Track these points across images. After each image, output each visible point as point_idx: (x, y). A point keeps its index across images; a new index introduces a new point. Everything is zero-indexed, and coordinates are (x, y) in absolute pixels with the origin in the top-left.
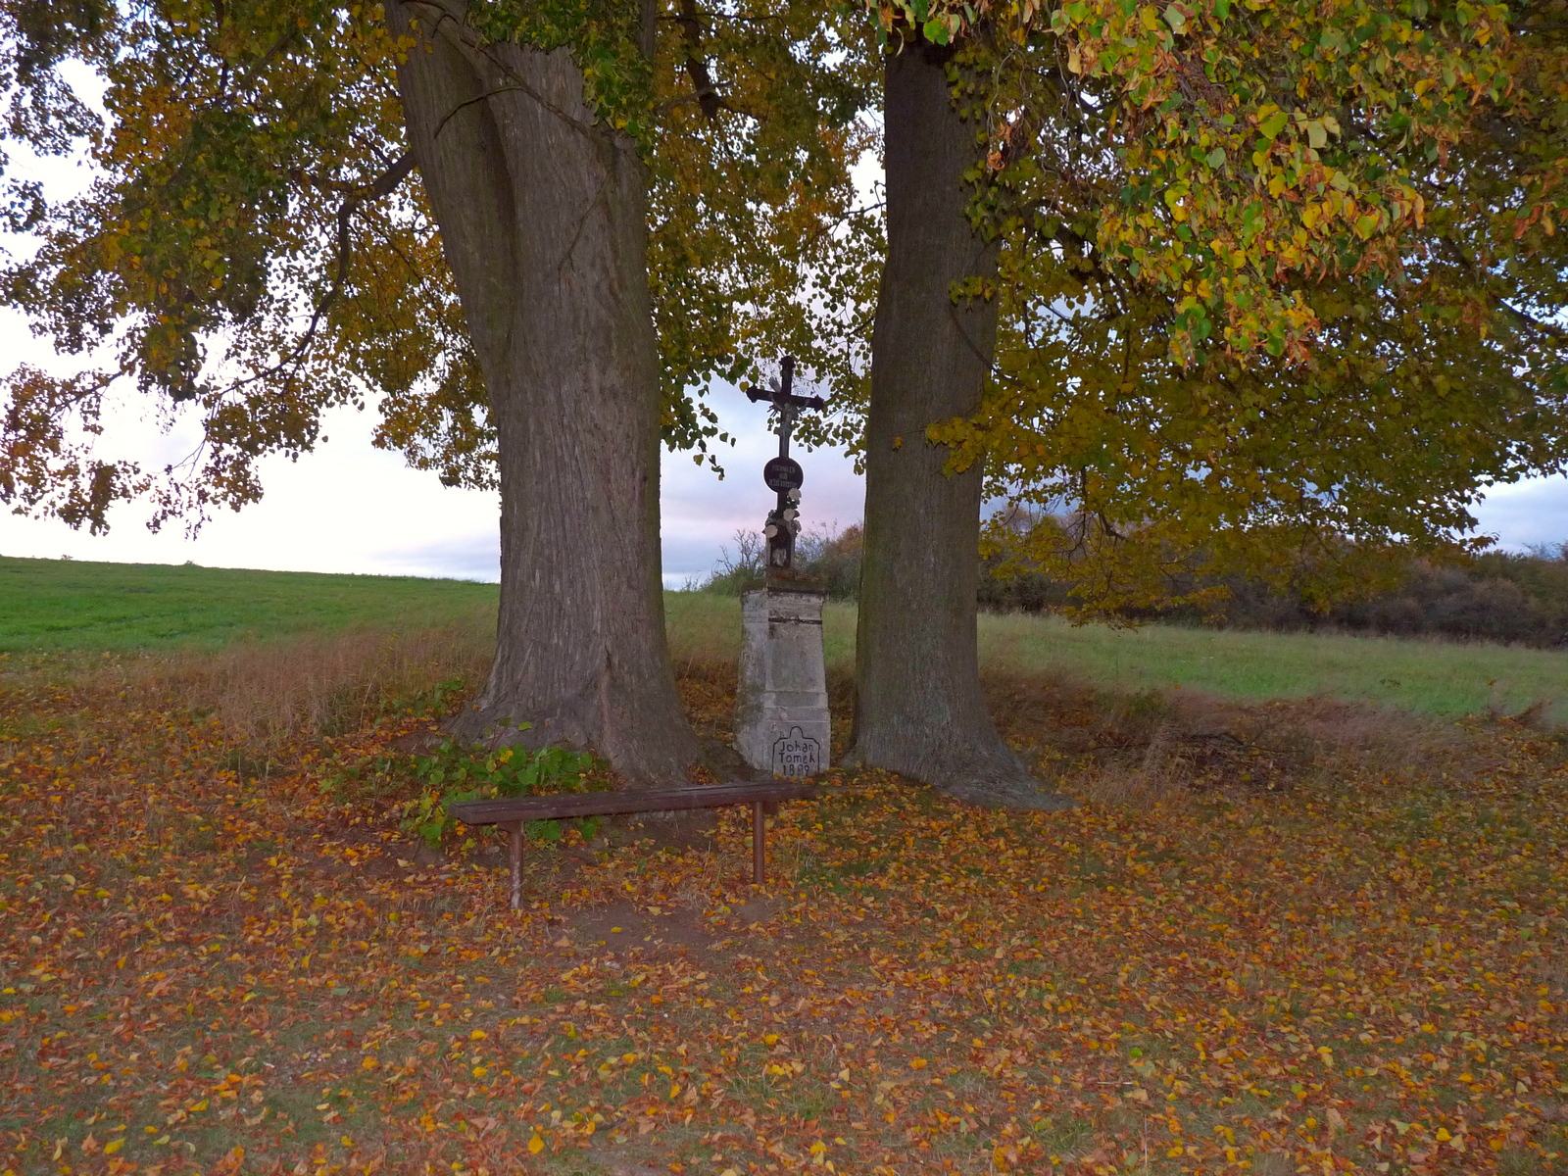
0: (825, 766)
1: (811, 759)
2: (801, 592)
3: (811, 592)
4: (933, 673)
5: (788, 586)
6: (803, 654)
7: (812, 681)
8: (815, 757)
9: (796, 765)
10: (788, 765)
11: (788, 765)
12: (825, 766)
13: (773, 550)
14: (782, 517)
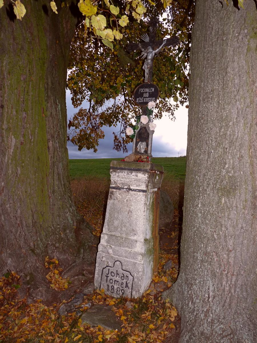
2: (131, 170)
3: (138, 170)
5: (122, 166)
6: (130, 212)
8: (130, 285)
9: (116, 287)
10: (110, 285)
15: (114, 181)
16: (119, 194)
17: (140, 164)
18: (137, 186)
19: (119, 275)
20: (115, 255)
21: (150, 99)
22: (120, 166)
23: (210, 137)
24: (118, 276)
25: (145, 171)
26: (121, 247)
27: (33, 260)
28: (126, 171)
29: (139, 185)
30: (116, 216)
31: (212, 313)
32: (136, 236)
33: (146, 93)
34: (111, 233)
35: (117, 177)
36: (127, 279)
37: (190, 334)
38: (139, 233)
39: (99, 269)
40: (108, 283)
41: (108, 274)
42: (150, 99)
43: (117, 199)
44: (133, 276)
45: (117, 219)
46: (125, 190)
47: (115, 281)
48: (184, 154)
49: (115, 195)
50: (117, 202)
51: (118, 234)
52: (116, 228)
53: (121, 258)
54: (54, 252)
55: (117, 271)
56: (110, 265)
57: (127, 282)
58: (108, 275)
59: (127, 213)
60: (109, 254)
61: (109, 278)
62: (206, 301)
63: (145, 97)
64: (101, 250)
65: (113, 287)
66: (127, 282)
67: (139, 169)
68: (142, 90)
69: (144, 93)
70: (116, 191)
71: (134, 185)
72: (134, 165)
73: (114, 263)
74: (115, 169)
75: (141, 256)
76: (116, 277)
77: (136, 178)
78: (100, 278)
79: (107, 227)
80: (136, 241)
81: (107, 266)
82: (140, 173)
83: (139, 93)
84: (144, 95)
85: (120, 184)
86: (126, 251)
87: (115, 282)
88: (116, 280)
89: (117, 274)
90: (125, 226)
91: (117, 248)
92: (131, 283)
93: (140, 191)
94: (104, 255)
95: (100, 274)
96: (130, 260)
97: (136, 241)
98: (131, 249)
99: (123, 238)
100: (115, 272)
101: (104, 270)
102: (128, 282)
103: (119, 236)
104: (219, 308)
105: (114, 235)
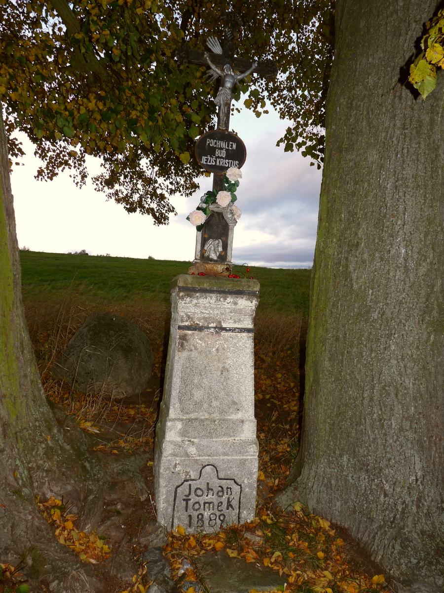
0: (248, 516)
1: (229, 505)
2: (224, 293)
3: (239, 293)
4: (398, 408)
6: (225, 370)
7: (236, 405)
8: (235, 503)
9: (206, 514)
10: (195, 514)
11: (195, 514)
12: (248, 516)
13: (204, 242)
14: (214, 202)
15: (186, 314)
16: (200, 340)
17: (241, 282)
18: (235, 322)
19: (212, 490)
20: (202, 456)
21: (229, 163)
22: (201, 286)
23: (409, 245)
24: (211, 492)
25: (251, 295)
26: (212, 438)
27: (25, 515)
28: (214, 296)
29: (240, 321)
30: (196, 381)
31: (426, 501)
32: (240, 412)
33: (221, 149)
34: (188, 416)
35: (189, 308)
36: (229, 493)
37: (399, 541)
38: (246, 406)
39: (168, 491)
40: (191, 511)
41: (190, 494)
42: (229, 163)
43: (196, 349)
44: (240, 485)
45: (199, 386)
46: (212, 330)
47: (205, 503)
48: (308, 265)
49: (191, 341)
50: (197, 354)
51: (203, 415)
52: (198, 405)
53: (216, 458)
54: (44, 483)
55: (208, 484)
56: (192, 477)
57: (229, 498)
58: (190, 497)
59: (220, 373)
60: (189, 457)
61: (191, 503)
62: (414, 487)
63: (219, 157)
64: (170, 452)
65: (200, 516)
66: (229, 498)
67: (239, 290)
68: (212, 143)
69: (216, 148)
70: (193, 333)
71: (230, 321)
72: (229, 284)
73: (201, 470)
74: (190, 291)
75: (254, 445)
76: (207, 496)
77: (234, 306)
78: (170, 510)
79: (177, 405)
80: (243, 422)
81: (187, 481)
82: (242, 298)
83: (207, 148)
84: (217, 153)
85: (199, 319)
86: (225, 444)
87: (204, 506)
88: (207, 501)
89: (209, 489)
90: (216, 398)
91: (205, 442)
92: (237, 498)
93: (242, 330)
94: (178, 460)
95: (172, 499)
96: (234, 457)
97: (243, 422)
98: (233, 438)
99: (215, 421)
100: (204, 487)
101: (179, 490)
102: (232, 497)
103: (207, 419)
104: (432, 491)
105: (196, 419)
